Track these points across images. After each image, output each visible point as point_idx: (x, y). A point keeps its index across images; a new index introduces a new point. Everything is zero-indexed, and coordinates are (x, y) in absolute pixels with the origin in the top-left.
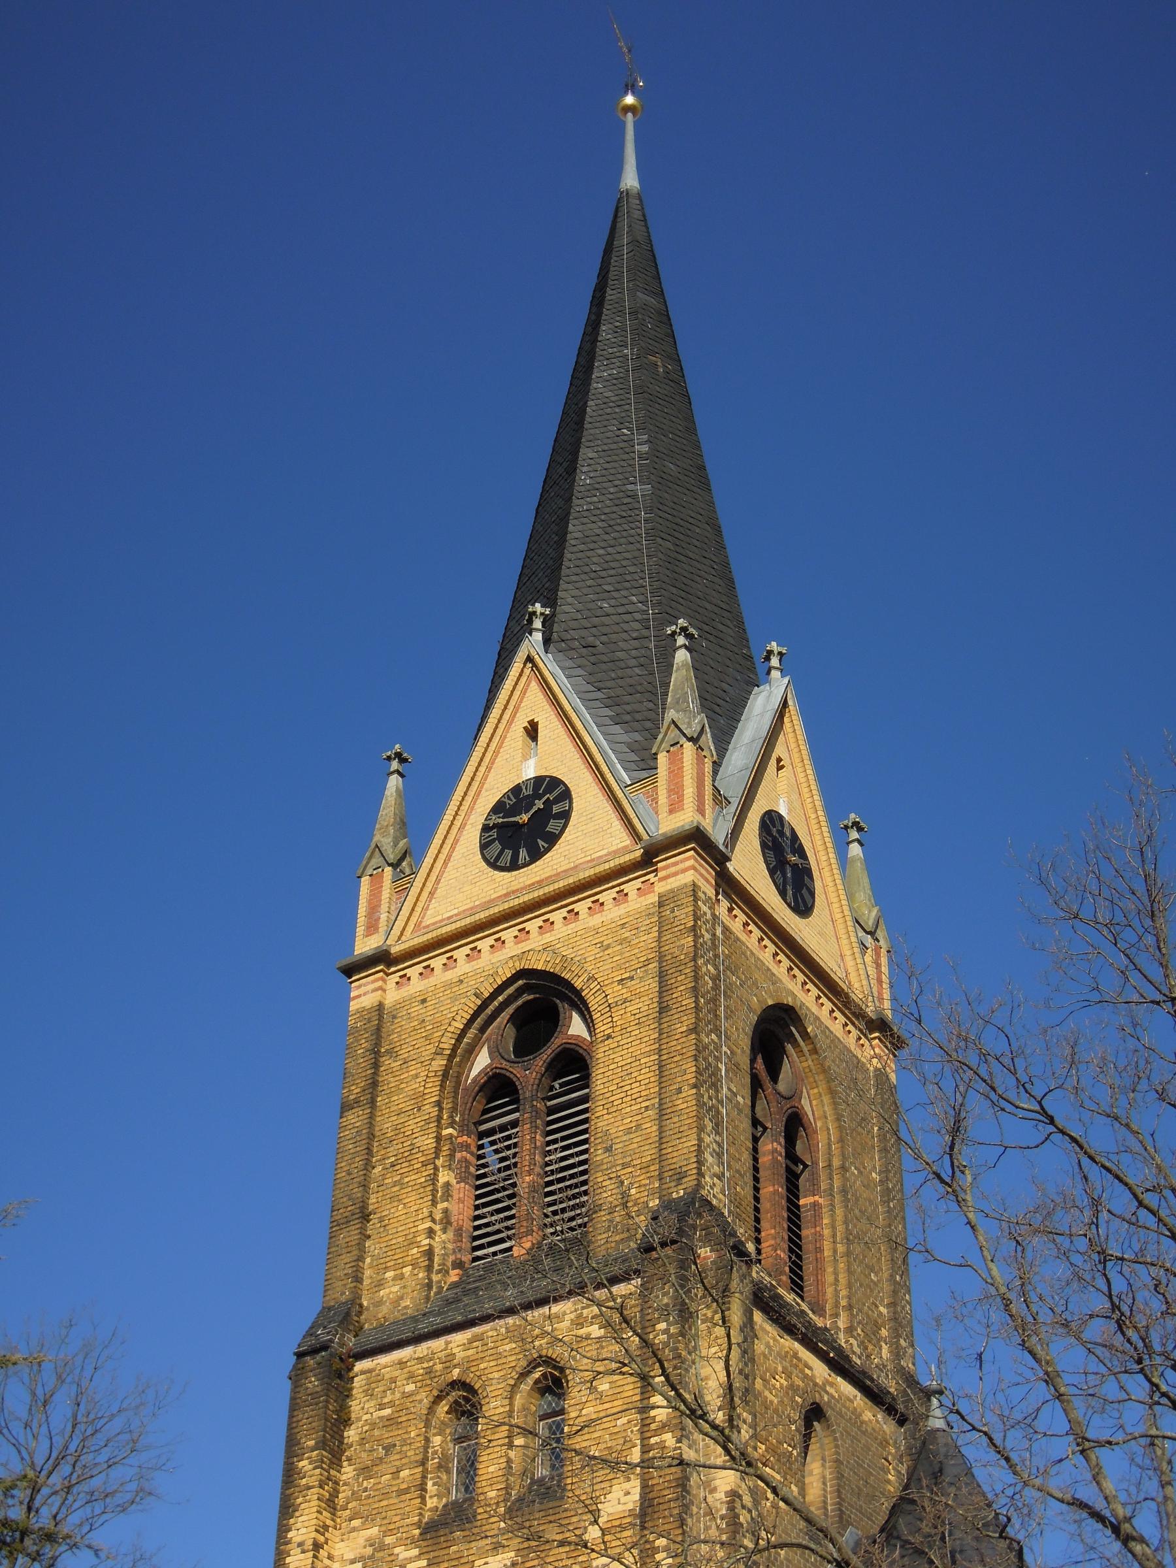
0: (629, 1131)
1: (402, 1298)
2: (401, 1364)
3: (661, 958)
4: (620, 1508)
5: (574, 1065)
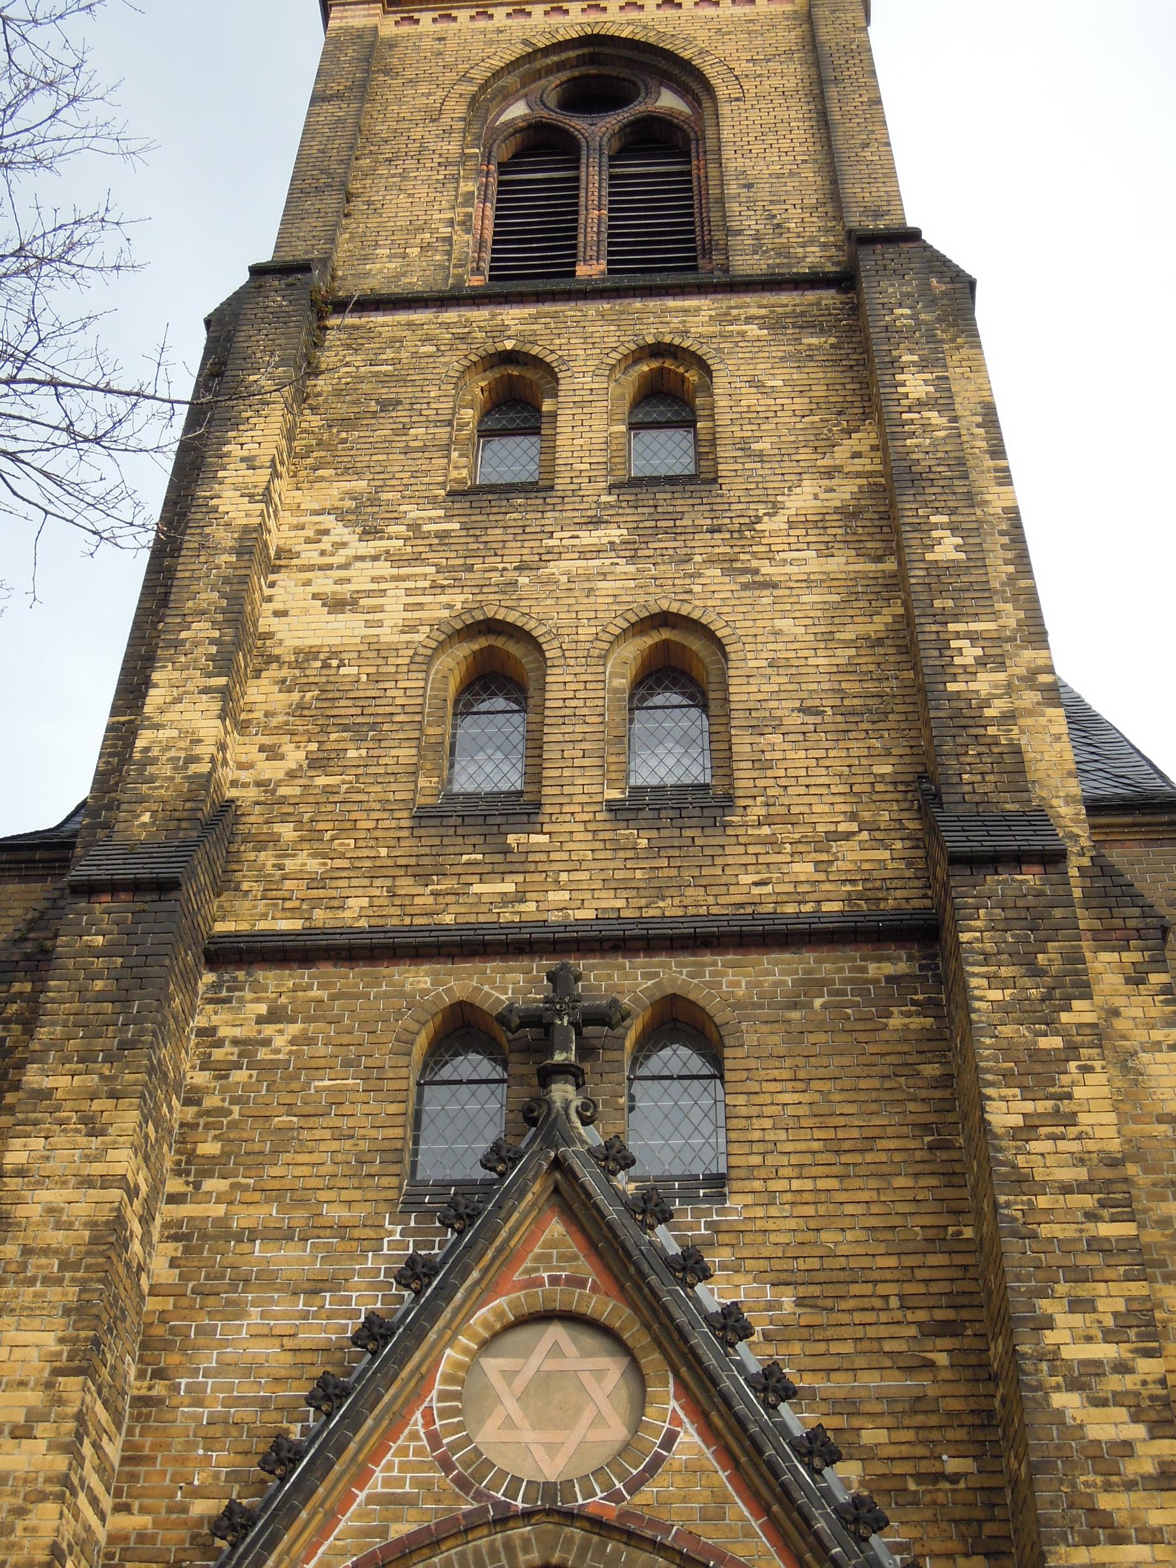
0: (779, 176)
1: (404, 274)
2: (410, 324)
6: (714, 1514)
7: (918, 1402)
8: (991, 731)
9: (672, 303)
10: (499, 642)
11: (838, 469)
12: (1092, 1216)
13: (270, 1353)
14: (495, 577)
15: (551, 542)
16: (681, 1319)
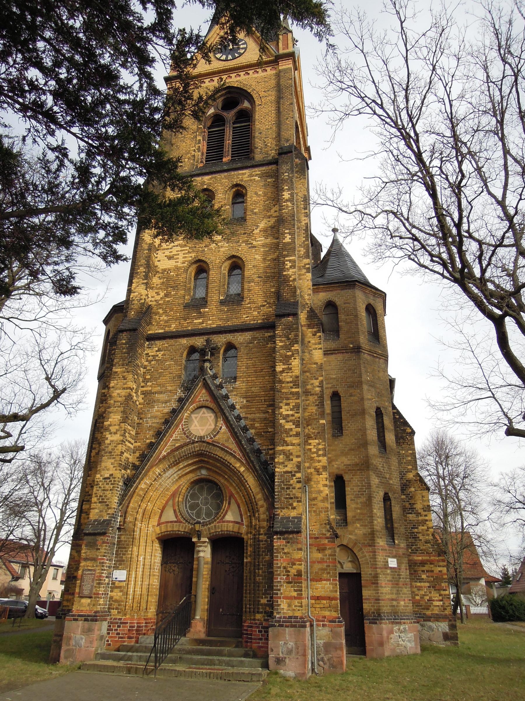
0: (268, 129)
6: (227, 441)
7: (265, 419)
9: (240, 172)
10: (202, 264)
11: (271, 215)
12: (292, 388)
13: (159, 413)
14: (201, 249)
16: (223, 407)
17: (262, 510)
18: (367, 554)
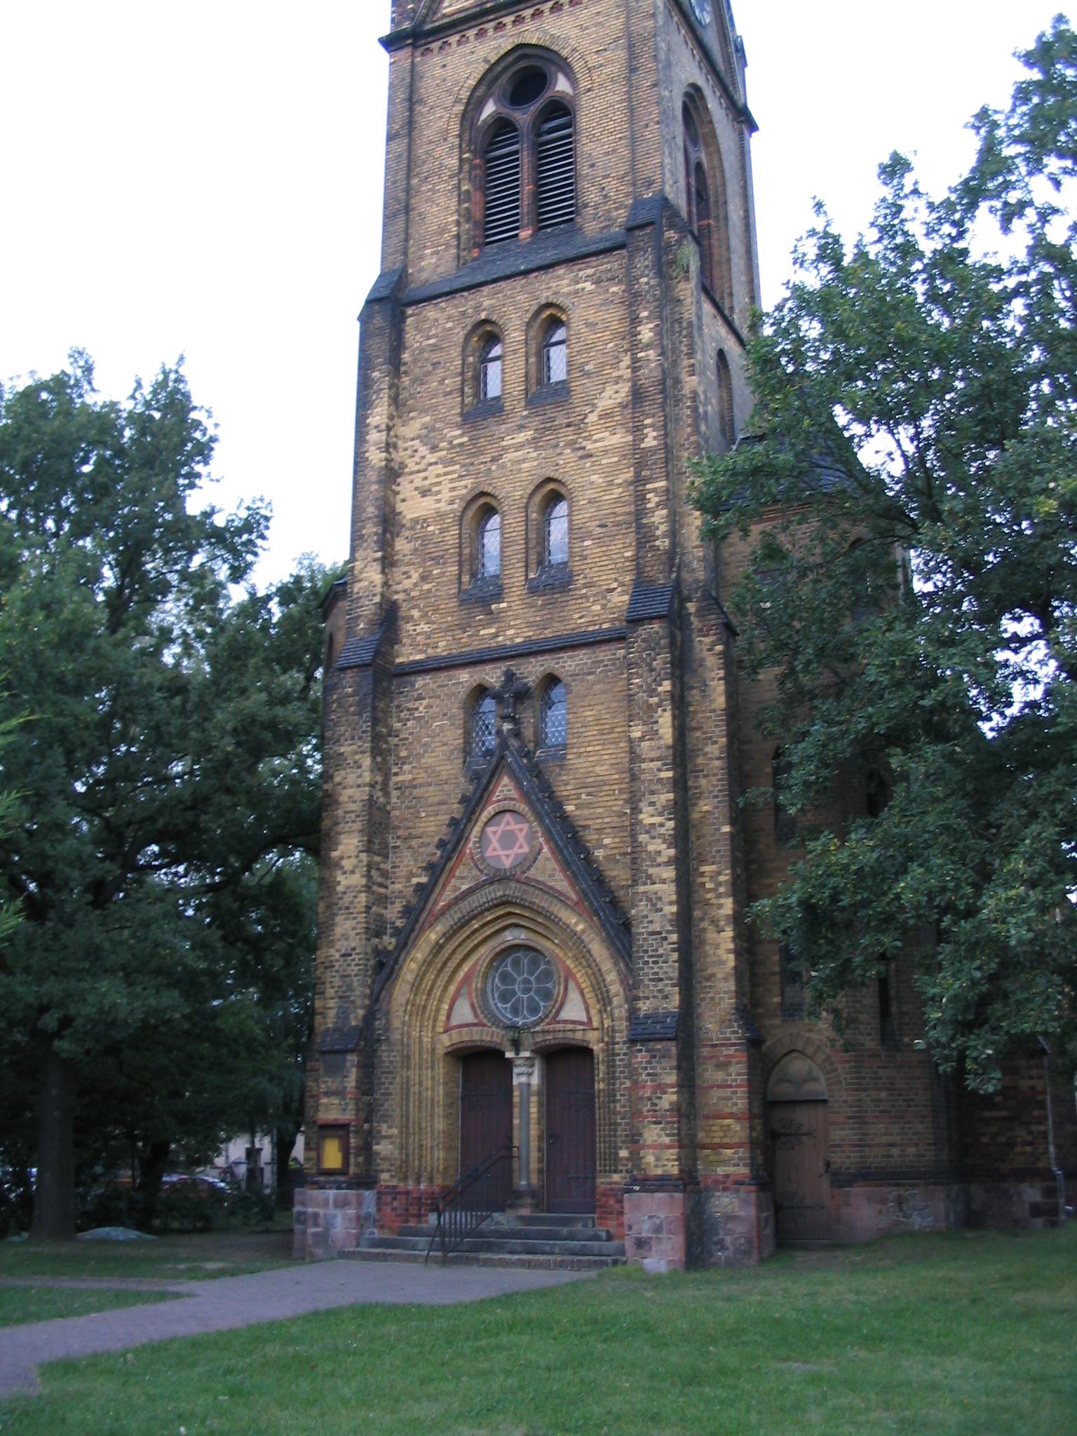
0: (607, 154)
3: (629, 36)
4: (611, 401)
5: (561, 110)
8: (657, 543)
11: (620, 377)
12: (659, 770)
14: (483, 468)
15: (504, 443)
17: (616, 1001)
18: (839, 1066)
